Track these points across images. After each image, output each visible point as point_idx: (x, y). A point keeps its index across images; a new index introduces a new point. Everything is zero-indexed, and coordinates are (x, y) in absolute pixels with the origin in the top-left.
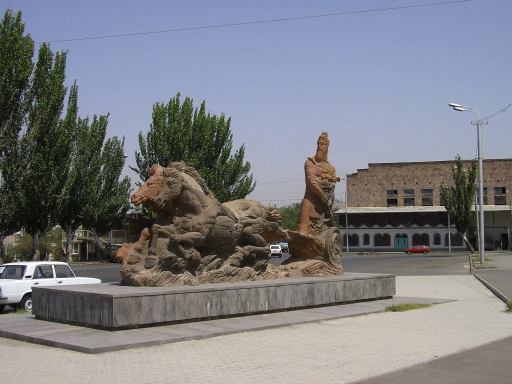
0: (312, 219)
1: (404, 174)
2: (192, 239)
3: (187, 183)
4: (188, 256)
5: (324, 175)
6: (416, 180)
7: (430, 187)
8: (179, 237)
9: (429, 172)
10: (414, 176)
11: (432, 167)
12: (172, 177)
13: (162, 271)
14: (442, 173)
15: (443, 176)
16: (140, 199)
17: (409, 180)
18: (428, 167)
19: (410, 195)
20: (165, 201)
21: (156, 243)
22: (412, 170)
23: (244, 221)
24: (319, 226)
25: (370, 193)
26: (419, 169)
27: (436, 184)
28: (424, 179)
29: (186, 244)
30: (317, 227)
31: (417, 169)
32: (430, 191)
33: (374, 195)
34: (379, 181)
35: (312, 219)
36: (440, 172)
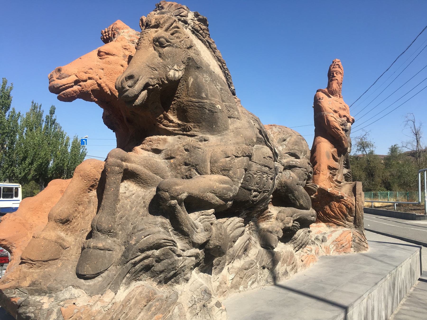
0: (330, 168)
2: (214, 192)
3: (198, 53)
4: (200, 237)
5: (342, 113)
8: (185, 187)
12: (166, 30)
13: (128, 284)
16: (76, 82)
20: (146, 86)
21: (116, 199)
23: (284, 161)
24: (339, 179)
29: (194, 203)
30: (336, 181)
35: (330, 168)
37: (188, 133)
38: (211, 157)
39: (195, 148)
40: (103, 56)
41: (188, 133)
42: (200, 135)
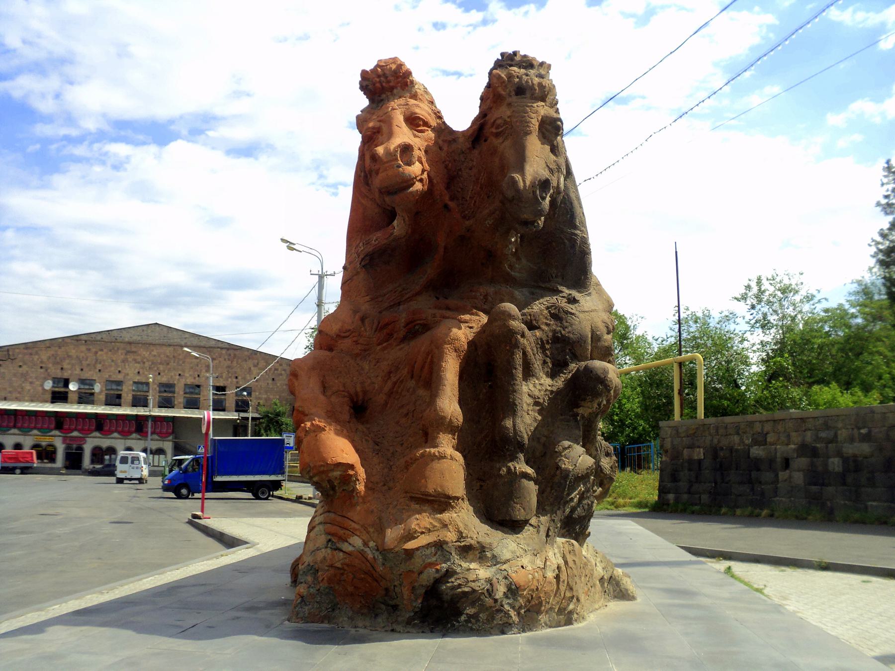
1: (82, 354)
6: (99, 366)
7: (120, 377)
9: (120, 355)
10: (97, 360)
11: (124, 349)
14: (139, 359)
15: (139, 363)
17: (88, 365)
18: (118, 349)
19: (87, 387)
22: (94, 350)
25: (26, 380)
26: (105, 350)
27: (128, 374)
28: (111, 366)
31: (102, 350)
32: (119, 383)
33: (31, 383)
34: (42, 362)
36: (136, 357)
37: (548, 285)
38: (593, 332)
39: (567, 312)
40: (419, 126)
41: (548, 285)
42: (566, 291)
